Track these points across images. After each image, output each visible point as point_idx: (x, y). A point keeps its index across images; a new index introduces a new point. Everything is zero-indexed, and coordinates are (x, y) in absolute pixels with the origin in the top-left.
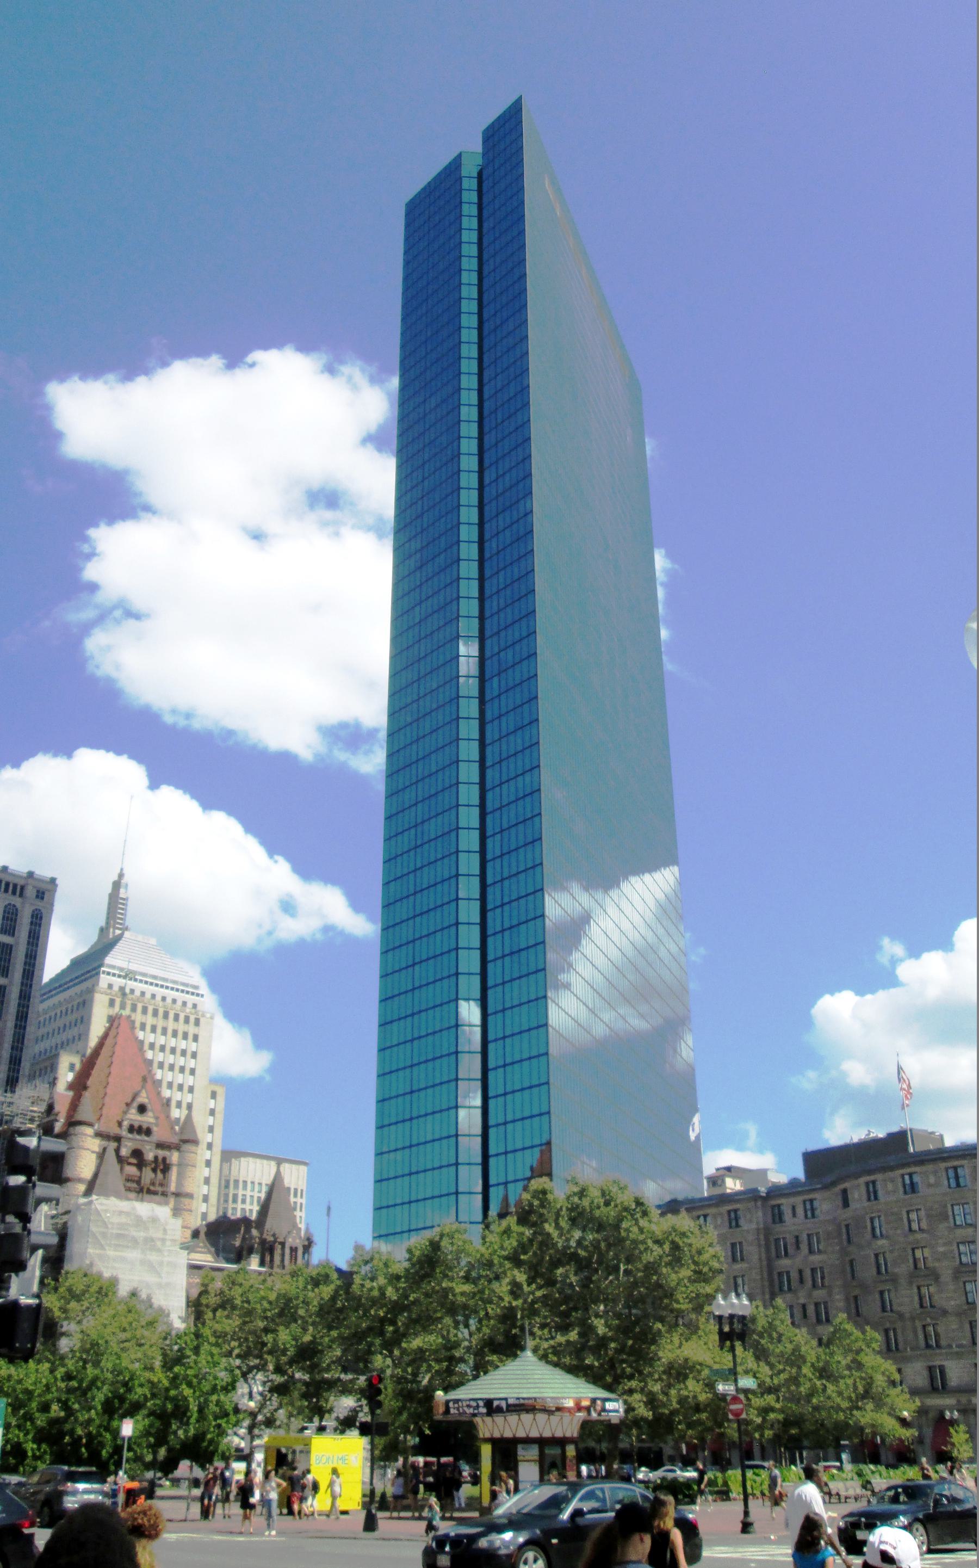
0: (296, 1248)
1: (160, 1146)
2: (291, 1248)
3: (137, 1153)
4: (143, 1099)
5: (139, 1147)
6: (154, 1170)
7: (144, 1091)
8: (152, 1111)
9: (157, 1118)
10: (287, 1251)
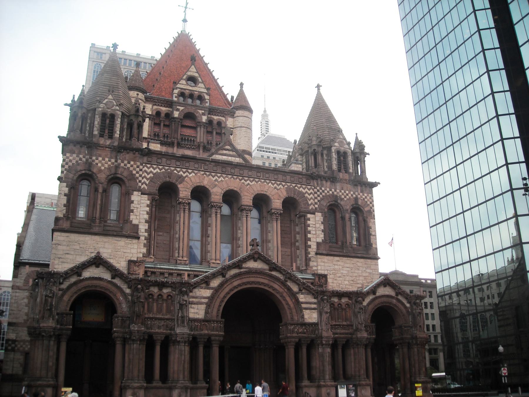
0: (345, 153)
1: (211, 111)
2: (338, 153)
3: (189, 116)
4: (192, 72)
5: (191, 110)
6: (210, 133)
7: (193, 66)
8: (202, 82)
9: (208, 89)
10: (334, 156)
